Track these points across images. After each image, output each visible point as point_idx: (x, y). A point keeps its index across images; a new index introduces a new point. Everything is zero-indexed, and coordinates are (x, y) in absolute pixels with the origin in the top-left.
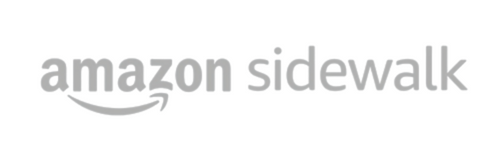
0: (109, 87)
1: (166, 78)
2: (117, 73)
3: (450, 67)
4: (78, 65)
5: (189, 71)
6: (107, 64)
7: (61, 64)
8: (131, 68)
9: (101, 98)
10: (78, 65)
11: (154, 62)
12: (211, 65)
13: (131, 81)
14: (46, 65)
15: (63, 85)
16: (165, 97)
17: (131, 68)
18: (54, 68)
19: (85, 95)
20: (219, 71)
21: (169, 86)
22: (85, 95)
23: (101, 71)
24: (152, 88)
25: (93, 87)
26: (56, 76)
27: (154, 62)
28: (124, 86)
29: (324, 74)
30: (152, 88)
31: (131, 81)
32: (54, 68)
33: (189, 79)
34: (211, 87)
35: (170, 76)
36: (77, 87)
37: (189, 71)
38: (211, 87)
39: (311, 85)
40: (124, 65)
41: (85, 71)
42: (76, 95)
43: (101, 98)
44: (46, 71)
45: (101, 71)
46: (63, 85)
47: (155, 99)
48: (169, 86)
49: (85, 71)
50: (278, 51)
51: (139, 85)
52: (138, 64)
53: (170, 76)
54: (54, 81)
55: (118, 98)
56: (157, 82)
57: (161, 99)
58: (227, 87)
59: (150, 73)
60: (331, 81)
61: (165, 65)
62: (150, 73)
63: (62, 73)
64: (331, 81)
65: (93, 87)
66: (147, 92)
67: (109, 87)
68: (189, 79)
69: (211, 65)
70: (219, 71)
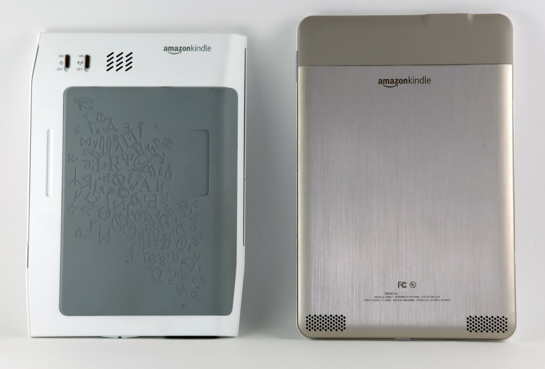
0: (389, 83)
1: (397, 82)
2: (390, 81)
3: (410, 79)
4: (384, 80)
5: (401, 81)
6: (388, 80)
9: (387, 85)
10: (384, 80)
12: (404, 80)
13: (392, 82)
14: (379, 80)
15: (382, 83)
16: (397, 85)
17: (392, 80)
18: (380, 80)
19: (385, 84)
21: (398, 83)
22: (385, 84)
23: (387, 81)
25: (386, 83)
26: (381, 82)
27: (396, 79)
29: (427, 81)
31: (392, 82)
32: (380, 80)
34: (404, 83)
36: (384, 83)
37: (401, 81)
38: (404, 83)
39: (423, 83)
40: (391, 80)
41: (385, 81)
42: (384, 85)
43: (387, 85)
45: (387, 81)
46: (382, 83)
49: (385, 81)
50: (413, 77)
51: (393, 83)
52: (393, 80)
54: (380, 82)
55: (390, 85)
56: (396, 82)
58: (407, 83)
59: (395, 81)
60: (429, 82)
61: (397, 80)
62: (395, 81)
64: (429, 82)
65: (386, 83)
66: (394, 84)
67: (389, 83)
69: (404, 80)
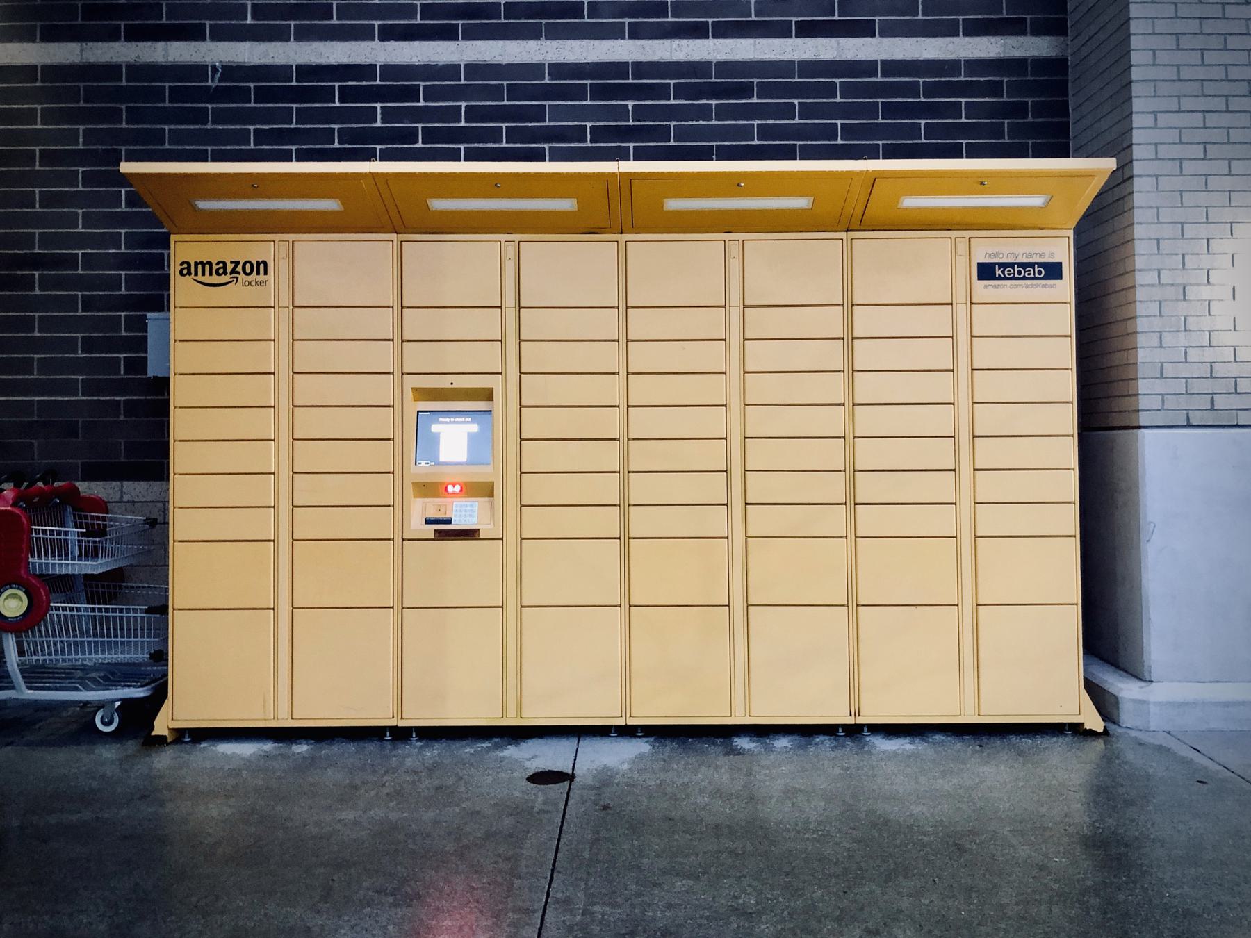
0: (211, 274)
1: (237, 270)
2: (215, 267)
4: (196, 264)
5: (248, 266)
6: (210, 263)
7: (189, 264)
8: (221, 265)
9: (207, 279)
11: (232, 262)
12: (259, 264)
14: (182, 264)
15: (189, 273)
16: (237, 278)
17: (221, 265)
18: (185, 265)
19: (200, 277)
20: (262, 266)
21: (239, 273)
22: (200, 277)
23: (207, 267)
24: (231, 274)
25: (203, 274)
27: (232, 262)
28: (218, 274)
30: (231, 274)
32: (185, 265)
33: (248, 271)
34: (258, 273)
35: (239, 269)
36: (196, 274)
37: (248, 266)
40: (218, 264)
41: (200, 266)
42: (196, 278)
43: (207, 279)
44: (181, 267)
45: (207, 267)
46: (189, 273)
47: (232, 279)
48: (239, 273)
49: (200, 266)
51: (225, 273)
52: (224, 263)
53: (239, 269)
54: (185, 272)
56: (233, 271)
57: (235, 279)
59: (230, 267)
61: (237, 263)
62: (230, 267)
63: (189, 268)
65: (203, 274)
67: (211, 274)
68: (248, 271)
70: (262, 266)
